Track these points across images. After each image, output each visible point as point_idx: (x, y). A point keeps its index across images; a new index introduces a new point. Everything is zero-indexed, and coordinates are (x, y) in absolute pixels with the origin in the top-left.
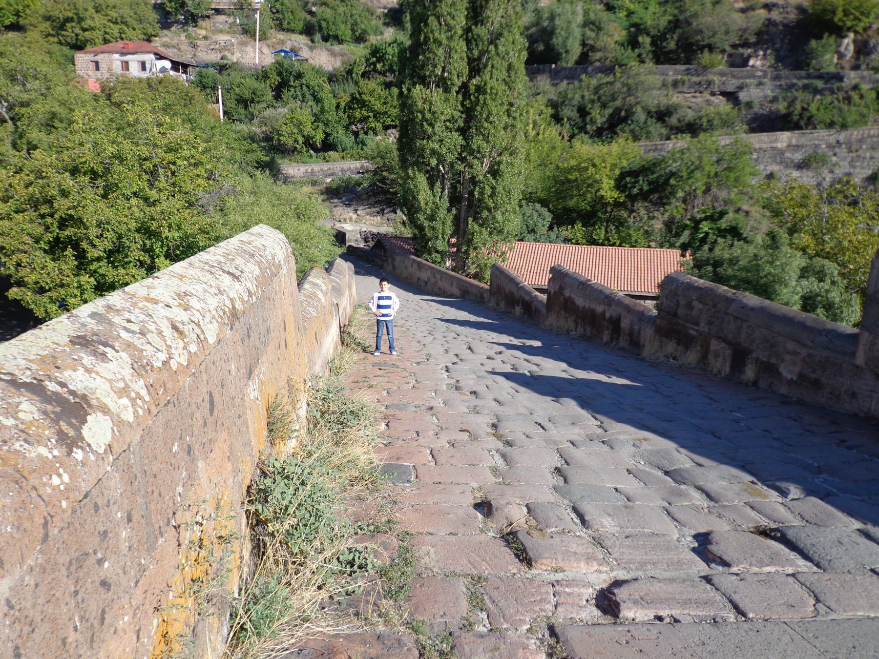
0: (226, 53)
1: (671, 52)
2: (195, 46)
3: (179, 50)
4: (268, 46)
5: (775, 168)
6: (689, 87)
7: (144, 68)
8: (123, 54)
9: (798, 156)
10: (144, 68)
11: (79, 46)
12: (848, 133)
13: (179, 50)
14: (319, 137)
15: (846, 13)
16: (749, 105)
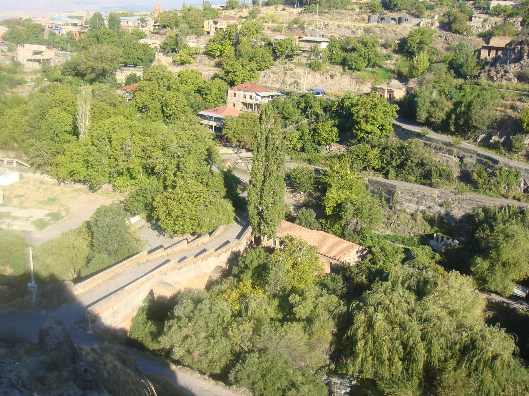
0: (298, 79)
1: (461, 125)
4: (320, 73)
5: (432, 204)
6: (446, 151)
7: (251, 98)
8: (244, 92)
9: (441, 201)
11: (232, 84)
12: (459, 196)
14: (299, 146)
16: (465, 165)
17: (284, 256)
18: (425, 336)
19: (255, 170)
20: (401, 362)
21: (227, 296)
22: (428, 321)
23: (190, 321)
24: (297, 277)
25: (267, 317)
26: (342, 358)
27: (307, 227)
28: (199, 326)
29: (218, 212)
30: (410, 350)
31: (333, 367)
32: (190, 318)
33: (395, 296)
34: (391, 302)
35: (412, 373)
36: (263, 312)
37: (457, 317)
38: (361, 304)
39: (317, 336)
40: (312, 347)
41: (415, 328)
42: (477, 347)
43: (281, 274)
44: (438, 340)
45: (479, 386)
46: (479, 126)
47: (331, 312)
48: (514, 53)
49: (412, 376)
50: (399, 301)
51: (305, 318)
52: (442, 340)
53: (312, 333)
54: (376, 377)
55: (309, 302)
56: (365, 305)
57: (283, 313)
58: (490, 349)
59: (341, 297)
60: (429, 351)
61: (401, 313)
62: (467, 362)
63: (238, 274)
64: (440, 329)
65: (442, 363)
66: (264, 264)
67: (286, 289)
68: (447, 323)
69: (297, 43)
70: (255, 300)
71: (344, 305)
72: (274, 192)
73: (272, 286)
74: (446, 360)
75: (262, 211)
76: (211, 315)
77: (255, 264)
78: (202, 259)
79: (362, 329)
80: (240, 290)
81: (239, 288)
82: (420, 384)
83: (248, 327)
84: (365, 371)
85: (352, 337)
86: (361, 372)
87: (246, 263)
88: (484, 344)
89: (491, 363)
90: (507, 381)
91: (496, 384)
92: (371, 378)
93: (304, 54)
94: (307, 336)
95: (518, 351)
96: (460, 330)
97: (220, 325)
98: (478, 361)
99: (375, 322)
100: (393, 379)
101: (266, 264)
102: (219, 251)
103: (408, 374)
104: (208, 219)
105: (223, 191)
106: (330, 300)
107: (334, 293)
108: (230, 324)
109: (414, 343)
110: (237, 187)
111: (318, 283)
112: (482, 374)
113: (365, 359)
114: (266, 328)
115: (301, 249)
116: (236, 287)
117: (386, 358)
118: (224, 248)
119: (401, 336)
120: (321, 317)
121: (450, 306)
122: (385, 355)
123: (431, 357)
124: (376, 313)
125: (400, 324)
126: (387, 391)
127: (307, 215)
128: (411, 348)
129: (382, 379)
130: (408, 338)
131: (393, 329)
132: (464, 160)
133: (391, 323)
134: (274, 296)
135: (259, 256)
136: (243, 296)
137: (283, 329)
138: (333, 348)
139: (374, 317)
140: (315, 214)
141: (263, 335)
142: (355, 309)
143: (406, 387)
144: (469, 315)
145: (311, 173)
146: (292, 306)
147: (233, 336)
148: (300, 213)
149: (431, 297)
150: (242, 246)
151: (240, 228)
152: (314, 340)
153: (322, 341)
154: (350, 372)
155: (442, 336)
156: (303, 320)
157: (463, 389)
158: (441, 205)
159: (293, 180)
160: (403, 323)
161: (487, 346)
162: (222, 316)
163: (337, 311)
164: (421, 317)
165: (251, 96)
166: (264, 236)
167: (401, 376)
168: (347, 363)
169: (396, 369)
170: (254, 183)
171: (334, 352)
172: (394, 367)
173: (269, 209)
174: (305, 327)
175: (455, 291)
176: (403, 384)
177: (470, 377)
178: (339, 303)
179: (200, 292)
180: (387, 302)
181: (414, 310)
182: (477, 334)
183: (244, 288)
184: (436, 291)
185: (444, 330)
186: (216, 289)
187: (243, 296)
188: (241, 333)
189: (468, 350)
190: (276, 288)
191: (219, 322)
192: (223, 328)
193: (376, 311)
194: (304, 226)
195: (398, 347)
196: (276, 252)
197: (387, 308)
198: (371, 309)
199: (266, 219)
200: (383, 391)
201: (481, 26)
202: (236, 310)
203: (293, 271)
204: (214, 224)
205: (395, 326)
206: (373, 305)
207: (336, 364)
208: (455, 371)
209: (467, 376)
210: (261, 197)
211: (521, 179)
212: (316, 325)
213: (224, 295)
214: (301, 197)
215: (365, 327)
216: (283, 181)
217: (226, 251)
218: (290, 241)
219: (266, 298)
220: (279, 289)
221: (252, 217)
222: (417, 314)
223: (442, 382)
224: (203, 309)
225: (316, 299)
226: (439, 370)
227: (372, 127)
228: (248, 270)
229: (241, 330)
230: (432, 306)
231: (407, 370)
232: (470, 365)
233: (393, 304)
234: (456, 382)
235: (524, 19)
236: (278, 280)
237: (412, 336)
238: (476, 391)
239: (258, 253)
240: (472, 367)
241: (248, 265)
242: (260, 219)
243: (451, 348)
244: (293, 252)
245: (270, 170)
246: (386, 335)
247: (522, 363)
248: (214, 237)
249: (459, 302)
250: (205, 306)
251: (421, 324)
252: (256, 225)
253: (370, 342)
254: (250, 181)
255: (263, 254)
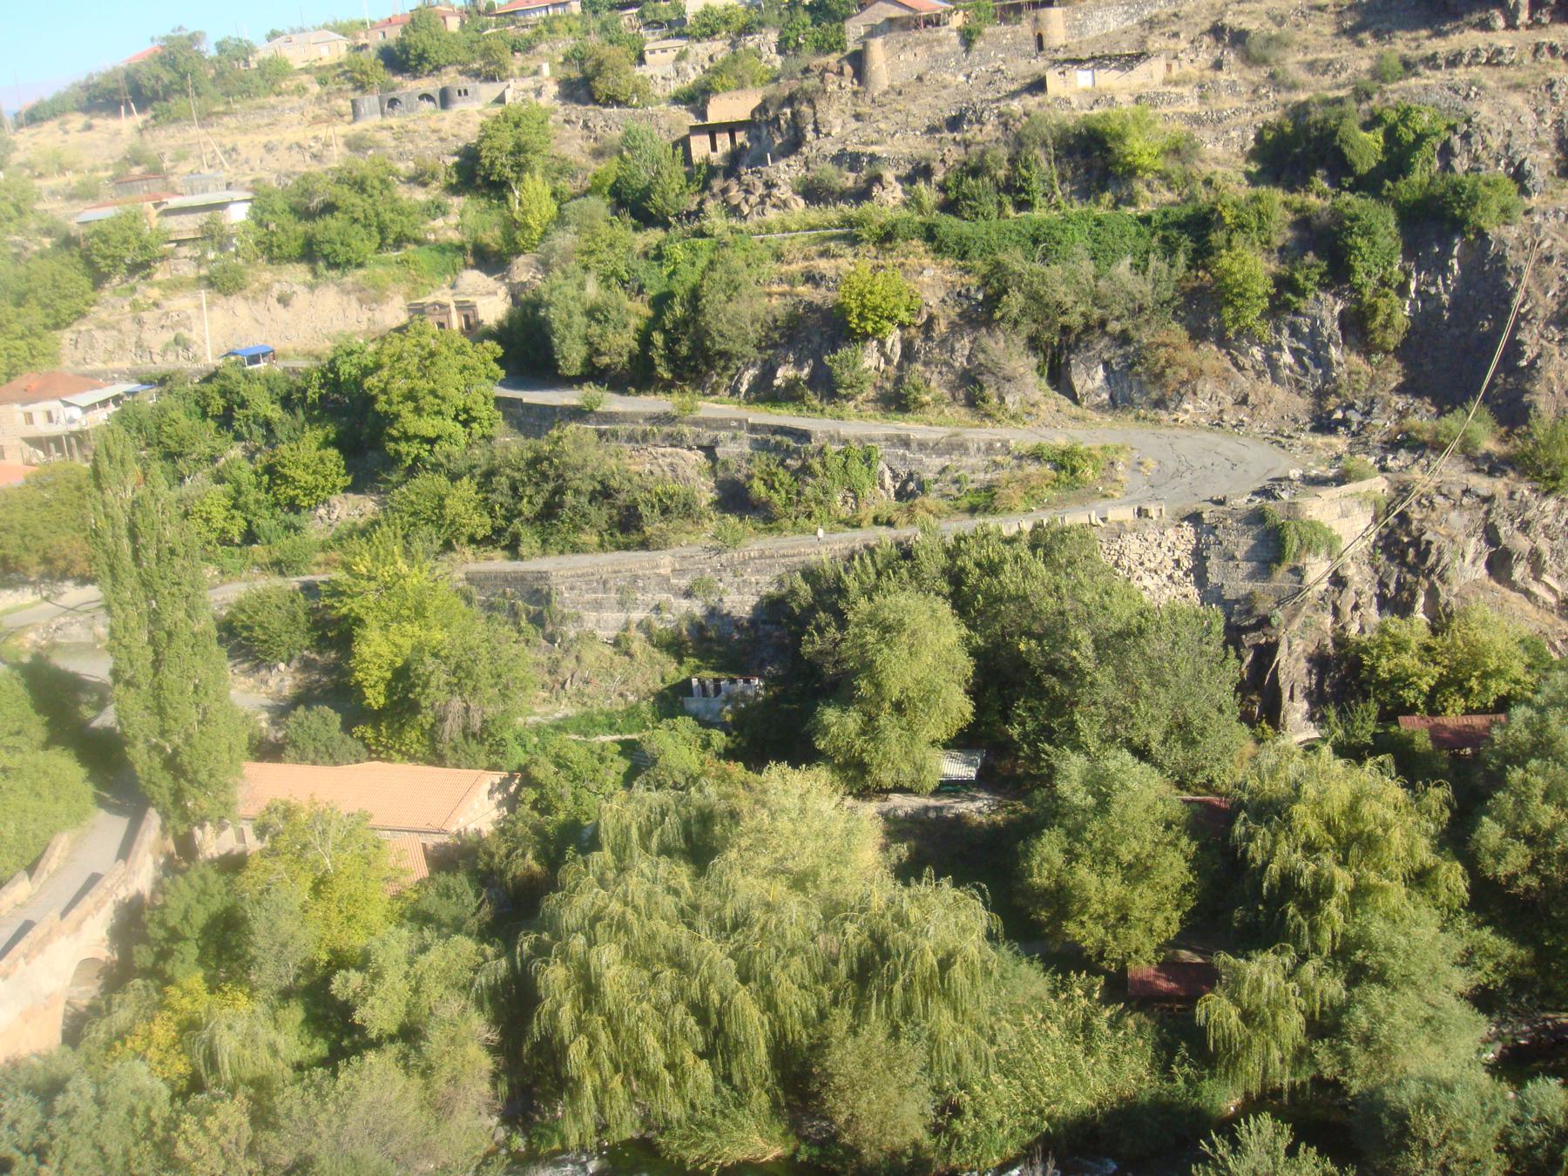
1: (687, 358)
2: (140, 322)
3: (120, 331)
4: (246, 299)
5: (664, 596)
6: (663, 440)
7: (50, 419)
8: (24, 404)
9: (684, 583)
10: (50, 419)
12: (729, 555)
13: (120, 331)
14: (236, 530)
15: (861, 317)
16: (725, 464)
17: (280, 866)
18: (748, 970)
19: (118, 634)
20: (704, 1064)
21: (139, 1044)
22: (744, 924)
23: (42, 1161)
24: (336, 919)
25: (281, 1065)
26: (537, 1110)
27: (324, 764)
28: (77, 1165)
29: (38, 795)
30: (720, 1021)
31: (519, 1142)
32: (40, 1153)
33: (635, 885)
34: (626, 904)
35: (744, 1080)
36: (264, 1055)
37: (817, 887)
38: (546, 936)
39: (446, 1072)
40: (441, 1109)
41: (714, 954)
42: (894, 952)
43: (286, 925)
44: (785, 967)
45: (929, 1053)
46: (734, 347)
47: (466, 988)
48: (779, 129)
49: (746, 1090)
50: (650, 895)
51: (394, 1029)
52: (797, 963)
53: (430, 1067)
54: (649, 1129)
55: (395, 983)
56: (557, 936)
57: (326, 1037)
58: (928, 945)
59: (485, 934)
60: (770, 1005)
61: (662, 927)
62: (879, 1001)
63: (155, 964)
64: (782, 937)
65: (813, 1026)
66: (227, 910)
67: (313, 963)
68: (797, 914)
69: (155, 224)
70: (230, 1027)
71: (497, 957)
72: (196, 687)
73: (269, 968)
74: (822, 1015)
75: (176, 752)
76: (106, 1117)
77: (200, 918)
78: (26, 956)
79: (567, 1006)
80: (175, 1011)
81: (169, 1007)
82: (775, 1105)
83: (233, 1113)
84: (613, 1124)
85: (546, 1040)
86: (602, 1128)
87: (171, 923)
88: (908, 938)
89: (942, 982)
90: (993, 1013)
91: (969, 1031)
92: (636, 1135)
93: (185, 251)
94: (418, 1081)
95: (998, 924)
96: (836, 920)
97: (145, 1138)
98: (907, 988)
99: (599, 976)
100: (698, 1116)
101: (234, 907)
102: (75, 914)
103: (734, 1088)
104: (12, 825)
105: (37, 728)
106: (452, 955)
107: (458, 930)
108: (173, 1124)
109: (723, 999)
110: (78, 703)
111: (402, 915)
112: (925, 1017)
113: (603, 1090)
114: (289, 1099)
115: (324, 832)
116: (161, 1006)
117: (661, 1066)
118: (88, 901)
119: (682, 990)
120: (444, 1013)
121: (790, 864)
122: (657, 1059)
123: (782, 1019)
124: (594, 950)
125: (669, 959)
126: (692, 1155)
127: (314, 726)
128: (719, 1014)
129: (666, 1127)
130: (704, 989)
131: (654, 978)
132: (719, 451)
133: (645, 962)
134: (286, 995)
135: (204, 892)
136: (190, 1026)
137: (341, 1086)
138: (503, 1088)
139: (593, 961)
140: (338, 718)
141: (284, 1122)
142: (530, 958)
143: (740, 1127)
144: (846, 872)
145: (293, 601)
146: (346, 1009)
147: (197, 1159)
148: (293, 726)
149: (732, 855)
150: (142, 876)
151: (120, 824)
152: (440, 1084)
153: (464, 1080)
154: (573, 1141)
155: (792, 952)
156: (392, 1039)
157: (890, 1076)
158: (688, 594)
159: (245, 634)
160: (678, 951)
161: (919, 940)
162: (141, 1108)
163: (481, 979)
164: (720, 919)
165: (49, 414)
166: (202, 827)
167: (717, 1101)
168: (556, 1119)
169: (698, 1087)
170: (127, 676)
171: (510, 1100)
172: (690, 1083)
173: (195, 740)
174: (405, 1057)
175: (791, 820)
176: (727, 1122)
177: (898, 1039)
178: (483, 954)
179: (48, 1059)
180: (616, 907)
181: (696, 908)
182: (883, 916)
183: (186, 1002)
184: (741, 835)
185: (794, 934)
186: (99, 1032)
187: (190, 1026)
188: (216, 1139)
189: (870, 968)
190: (282, 971)
191: (139, 1129)
192: (155, 1145)
193: (591, 942)
194: (314, 763)
195: (683, 1025)
196: (253, 863)
197: (622, 926)
198: (578, 942)
199: (196, 772)
200: (682, 1161)
201: (674, 74)
202: (181, 1076)
203: (321, 905)
204: (35, 836)
205: (658, 967)
206: (580, 929)
207: (526, 1133)
208: (856, 1034)
209: (889, 1037)
210: (161, 712)
211: (882, 466)
212: (435, 1041)
213: (129, 1044)
214: (283, 679)
215: (575, 998)
216: (214, 648)
217: (98, 906)
218: (285, 818)
219: (261, 1008)
220: (293, 971)
221: (149, 781)
222: (708, 915)
223: (832, 1076)
224: (75, 1109)
225: (411, 963)
226: (812, 1048)
227: (438, 421)
228: (181, 944)
229: (215, 1130)
230: (744, 880)
231: (727, 1078)
232: (889, 1005)
233: (636, 908)
234: (866, 1064)
235: (781, 33)
236: (284, 945)
237: (711, 979)
238: (924, 1069)
239: (198, 883)
240: (897, 1008)
241: (179, 927)
242: (175, 778)
243: (825, 977)
244: (304, 847)
245: (168, 624)
246: (640, 1001)
247: (1017, 953)
248: (45, 875)
249: (811, 845)
250: (79, 1095)
251: (728, 938)
252: (168, 799)
253: (603, 1037)
254: (115, 673)
255: (216, 883)
